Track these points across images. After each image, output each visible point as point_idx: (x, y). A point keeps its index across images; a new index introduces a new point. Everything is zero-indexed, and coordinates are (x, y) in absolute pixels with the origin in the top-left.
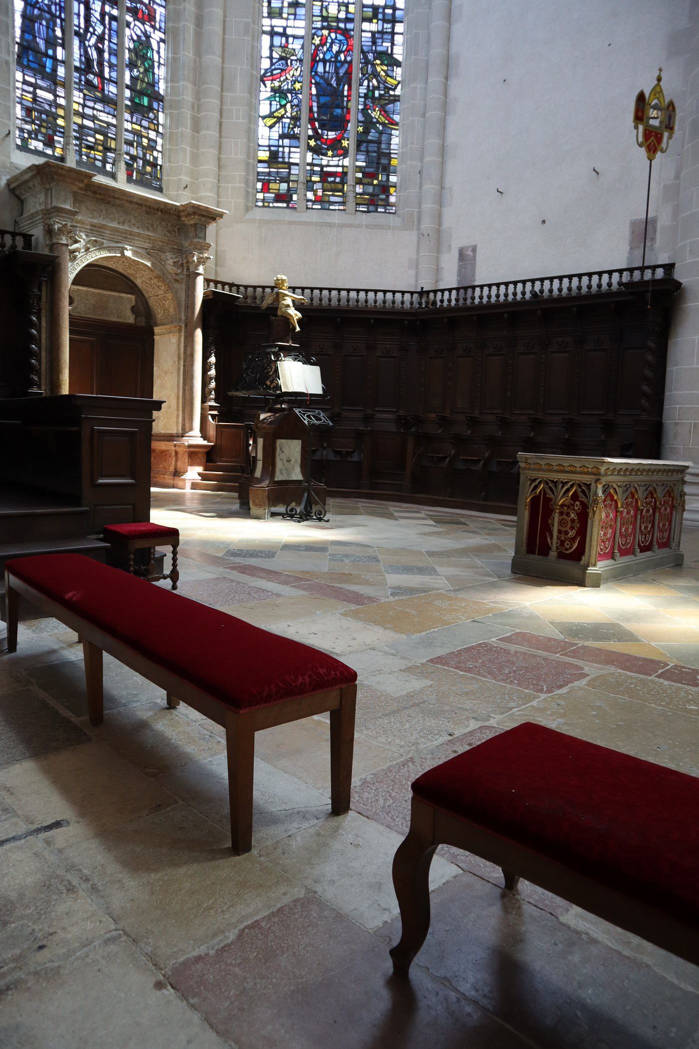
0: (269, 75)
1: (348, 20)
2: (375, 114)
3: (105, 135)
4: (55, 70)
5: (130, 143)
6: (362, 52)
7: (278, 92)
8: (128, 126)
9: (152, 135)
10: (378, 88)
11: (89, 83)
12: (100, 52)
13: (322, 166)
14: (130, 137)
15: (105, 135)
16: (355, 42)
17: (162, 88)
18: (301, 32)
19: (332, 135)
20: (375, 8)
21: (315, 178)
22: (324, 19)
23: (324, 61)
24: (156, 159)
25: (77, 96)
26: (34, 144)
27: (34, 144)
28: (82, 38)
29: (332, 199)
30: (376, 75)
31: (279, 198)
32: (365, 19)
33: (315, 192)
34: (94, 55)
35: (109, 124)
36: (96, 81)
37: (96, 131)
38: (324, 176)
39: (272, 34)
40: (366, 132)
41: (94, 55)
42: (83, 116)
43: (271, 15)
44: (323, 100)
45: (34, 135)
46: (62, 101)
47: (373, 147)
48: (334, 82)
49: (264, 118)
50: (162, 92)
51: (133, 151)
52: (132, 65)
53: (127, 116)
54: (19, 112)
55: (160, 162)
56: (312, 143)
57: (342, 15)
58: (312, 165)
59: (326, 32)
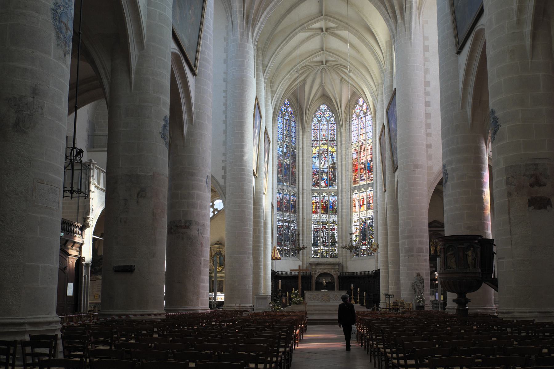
0: (355, 233)
1: (366, 221)
2: (371, 237)
3: (327, 251)
4: (318, 244)
5: (331, 251)
6: (368, 226)
7: (356, 236)
8: (331, 249)
9: (335, 248)
10: (371, 232)
11: (324, 244)
12: (325, 239)
13: (363, 248)
14: (331, 250)
15: (327, 251)
16: (366, 225)
17: (337, 240)
18: (359, 225)
19: (364, 242)
20: (370, 218)
21: (362, 250)
22: (362, 221)
23: (362, 229)
24: (336, 252)
25: (322, 247)
26: (315, 256)
27: (315, 256)
28: (322, 238)
29: (365, 254)
30: (370, 230)
31: (357, 255)
32: (368, 220)
33: (362, 253)
34: (324, 240)
35: (327, 249)
36: (325, 244)
37: (325, 251)
38: (363, 250)
39: (355, 226)
40: (369, 241)
41: (324, 240)
42: (323, 250)
43: (354, 223)
44: (363, 236)
45: (315, 255)
46: (319, 249)
47: (370, 243)
48: (364, 233)
49: (354, 241)
50: (337, 241)
51: (332, 252)
52: (331, 239)
53: (330, 247)
54: (313, 252)
55: (337, 253)
56: (361, 244)
57: (365, 220)
58: (362, 248)
59: (362, 224)
